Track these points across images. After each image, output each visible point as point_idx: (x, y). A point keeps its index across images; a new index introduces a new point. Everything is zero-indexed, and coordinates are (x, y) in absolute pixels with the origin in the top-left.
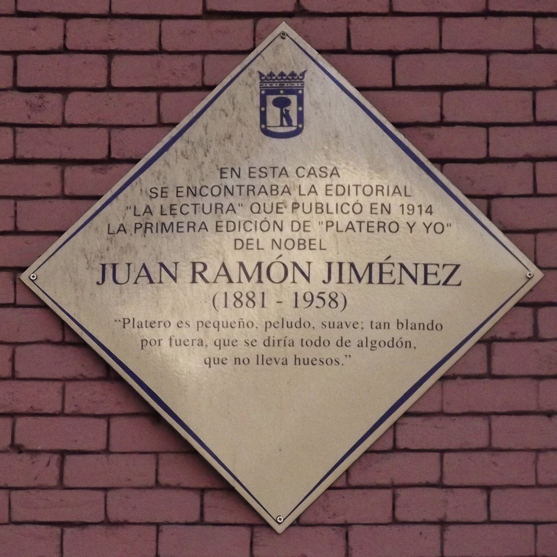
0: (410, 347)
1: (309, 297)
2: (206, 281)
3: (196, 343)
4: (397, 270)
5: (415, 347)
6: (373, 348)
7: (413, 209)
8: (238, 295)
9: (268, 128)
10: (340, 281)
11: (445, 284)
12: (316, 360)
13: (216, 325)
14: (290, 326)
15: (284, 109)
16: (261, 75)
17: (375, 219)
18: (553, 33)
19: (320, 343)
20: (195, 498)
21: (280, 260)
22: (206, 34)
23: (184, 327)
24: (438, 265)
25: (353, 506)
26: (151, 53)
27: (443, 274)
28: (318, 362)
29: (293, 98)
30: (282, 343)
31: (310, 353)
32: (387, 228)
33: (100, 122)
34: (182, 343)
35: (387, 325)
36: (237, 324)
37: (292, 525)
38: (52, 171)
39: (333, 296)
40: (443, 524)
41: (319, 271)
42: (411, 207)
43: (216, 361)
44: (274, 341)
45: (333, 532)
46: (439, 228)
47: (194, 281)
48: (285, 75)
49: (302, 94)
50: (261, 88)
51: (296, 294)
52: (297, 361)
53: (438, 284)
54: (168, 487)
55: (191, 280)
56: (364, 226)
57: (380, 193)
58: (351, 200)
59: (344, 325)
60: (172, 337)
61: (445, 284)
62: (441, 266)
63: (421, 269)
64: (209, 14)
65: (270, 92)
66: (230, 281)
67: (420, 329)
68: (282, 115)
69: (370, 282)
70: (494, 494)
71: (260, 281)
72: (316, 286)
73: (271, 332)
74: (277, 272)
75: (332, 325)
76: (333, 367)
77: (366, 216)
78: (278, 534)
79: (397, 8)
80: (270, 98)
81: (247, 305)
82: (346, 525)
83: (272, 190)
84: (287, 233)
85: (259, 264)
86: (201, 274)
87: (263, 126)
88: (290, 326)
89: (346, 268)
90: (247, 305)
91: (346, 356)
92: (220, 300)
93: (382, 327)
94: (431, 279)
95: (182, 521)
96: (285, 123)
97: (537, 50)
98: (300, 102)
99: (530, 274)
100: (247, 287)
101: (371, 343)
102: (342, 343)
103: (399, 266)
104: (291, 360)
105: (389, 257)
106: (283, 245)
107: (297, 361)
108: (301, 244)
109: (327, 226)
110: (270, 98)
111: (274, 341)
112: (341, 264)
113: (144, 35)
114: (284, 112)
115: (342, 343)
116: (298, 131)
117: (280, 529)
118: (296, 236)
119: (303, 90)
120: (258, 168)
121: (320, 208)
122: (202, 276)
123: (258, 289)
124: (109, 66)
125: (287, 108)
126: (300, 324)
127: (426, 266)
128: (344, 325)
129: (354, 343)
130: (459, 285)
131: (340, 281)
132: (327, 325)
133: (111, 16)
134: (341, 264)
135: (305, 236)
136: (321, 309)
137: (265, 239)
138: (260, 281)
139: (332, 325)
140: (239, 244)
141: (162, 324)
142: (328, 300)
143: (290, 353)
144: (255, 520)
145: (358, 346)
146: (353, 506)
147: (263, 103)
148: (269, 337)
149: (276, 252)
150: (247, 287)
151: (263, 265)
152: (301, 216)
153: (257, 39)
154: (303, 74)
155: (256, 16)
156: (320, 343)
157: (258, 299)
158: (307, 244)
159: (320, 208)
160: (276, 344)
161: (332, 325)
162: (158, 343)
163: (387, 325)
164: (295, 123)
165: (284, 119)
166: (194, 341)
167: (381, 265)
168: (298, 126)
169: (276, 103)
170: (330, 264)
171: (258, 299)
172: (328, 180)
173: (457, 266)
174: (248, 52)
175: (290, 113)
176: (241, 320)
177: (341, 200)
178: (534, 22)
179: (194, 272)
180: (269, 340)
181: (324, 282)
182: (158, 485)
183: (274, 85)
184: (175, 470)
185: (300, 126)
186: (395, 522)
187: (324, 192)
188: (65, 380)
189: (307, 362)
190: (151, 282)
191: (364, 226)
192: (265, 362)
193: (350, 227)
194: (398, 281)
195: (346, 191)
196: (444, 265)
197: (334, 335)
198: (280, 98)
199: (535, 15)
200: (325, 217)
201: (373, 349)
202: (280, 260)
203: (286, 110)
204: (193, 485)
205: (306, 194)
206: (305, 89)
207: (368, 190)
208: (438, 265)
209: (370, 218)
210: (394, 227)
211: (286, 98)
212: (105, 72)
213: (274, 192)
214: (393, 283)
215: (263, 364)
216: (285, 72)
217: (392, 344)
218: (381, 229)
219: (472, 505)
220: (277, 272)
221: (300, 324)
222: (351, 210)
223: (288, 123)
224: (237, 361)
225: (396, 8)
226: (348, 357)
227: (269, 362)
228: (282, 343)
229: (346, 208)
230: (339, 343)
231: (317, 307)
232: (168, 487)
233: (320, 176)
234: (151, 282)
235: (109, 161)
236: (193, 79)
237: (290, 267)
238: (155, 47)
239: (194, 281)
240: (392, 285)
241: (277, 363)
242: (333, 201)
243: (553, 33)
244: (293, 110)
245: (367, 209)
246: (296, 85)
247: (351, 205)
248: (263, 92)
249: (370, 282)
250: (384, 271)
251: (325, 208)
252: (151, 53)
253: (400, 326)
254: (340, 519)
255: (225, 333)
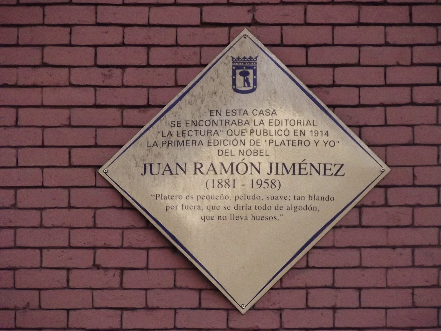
1: (259, 182)
2: (202, 173)
3: (196, 208)
7: (318, 133)
8: (220, 181)
10: (277, 173)
11: (335, 175)
13: (208, 198)
14: (249, 198)
16: (233, 58)
17: (297, 138)
19: (266, 208)
21: (243, 161)
24: (332, 164)
28: (265, 218)
29: (251, 71)
30: (244, 208)
31: (260, 213)
33: (143, 85)
35: (303, 198)
36: (220, 197)
38: (116, 112)
39: (273, 181)
40: (334, 309)
41: (265, 168)
42: (316, 132)
43: (208, 218)
45: (273, 313)
46: (332, 144)
47: (195, 173)
48: (246, 58)
49: (256, 69)
50: (233, 66)
51: (252, 180)
52: (253, 218)
53: (332, 175)
54: (181, 288)
55: (194, 173)
56: (290, 142)
57: (299, 124)
58: (283, 128)
59: (279, 198)
61: (335, 175)
62: (333, 165)
66: (216, 173)
68: (245, 81)
69: (294, 174)
70: (363, 292)
71: (232, 173)
72: (264, 176)
73: (239, 202)
74: (242, 168)
75: (272, 198)
76: (273, 221)
78: (242, 314)
80: (238, 71)
83: (239, 122)
85: (232, 164)
87: (234, 87)
88: (249, 198)
89: (280, 166)
92: (210, 184)
93: (301, 199)
94: (328, 172)
95: (189, 307)
96: (246, 85)
97: (387, 44)
98: (255, 73)
100: (225, 176)
102: (278, 208)
103: (310, 165)
104: (250, 218)
105: (304, 160)
107: (253, 218)
108: (255, 153)
109: (270, 143)
110: (238, 71)
112: (277, 164)
115: (278, 208)
116: (254, 90)
117: (243, 311)
118: (252, 148)
119: (256, 67)
120: (231, 110)
121: (266, 133)
122: (200, 171)
123: (231, 178)
124: (148, 54)
125: (248, 77)
127: (325, 165)
128: (279, 198)
130: (344, 175)
131: (277, 173)
134: (277, 164)
135: (258, 148)
137: (235, 150)
138: (232, 173)
139: (272, 198)
140: (221, 153)
141: (177, 197)
142: (270, 184)
143: (249, 213)
144: (229, 307)
147: (234, 74)
149: (242, 157)
150: (225, 176)
152: (255, 137)
153: (230, 38)
154: (256, 58)
155: (230, 25)
156: (266, 208)
157: (231, 183)
158: (259, 152)
159: (266, 133)
160: (241, 208)
161: (272, 198)
162: (175, 208)
163: (303, 198)
164: (252, 85)
165: (246, 83)
167: (300, 164)
168: (253, 87)
169: (241, 74)
170: (271, 164)
171: (231, 183)
173: (342, 165)
174: (225, 46)
175: (249, 80)
177: (277, 128)
178: (385, 29)
179: (196, 168)
181: (268, 174)
183: (240, 64)
184: (185, 279)
185: (255, 87)
186: (308, 307)
188: (123, 229)
189: (258, 218)
190: (172, 174)
191: (290, 142)
192: (235, 219)
193: (283, 143)
194: (309, 173)
195: (280, 123)
196: (335, 165)
197: (274, 203)
199: (386, 25)
200: (268, 138)
202: (243, 161)
204: (195, 287)
205: (258, 124)
206: (257, 66)
207: (292, 122)
208: (332, 164)
210: (307, 143)
212: (146, 57)
213: (240, 124)
214: (307, 174)
217: (306, 208)
218: (300, 144)
220: (242, 168)
221: (255, 197)
222: (283, 134)
224: (220, 218)
227: (237, 219)
228: (244, 208)
229: (280, 133)
230: (277, 208)
232: (181, 288)
233: (266, 115)
234: (172, 174)
235: (148, 106)
236: (195, 60)
237: (249, 165)
238: (173, 43)
239: (195, 173)
242: (273, 129)
244: (251, 78)
245: (292, 133)
246: (252, 64)
247: (283, 131)
249: (294, 174)
251: (268, 132)
253: (311, 198)
254: (277, 306)
255: (213, 202)
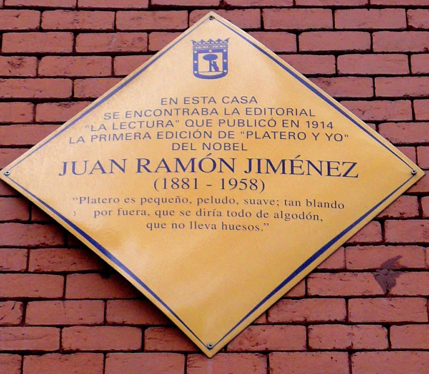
0: (318, 219)
1: (233, 182)
2: (149, 171)
3: (139, 213)
4: (305, 165)
5: (322, 220)
6: (287, 219)
7: (317, 125)
8: (175, 181)
9: (199, 73)
10: (259, 172)
11: (345, 175)
12: (240, 226)
13: (157, 201)
14: (218, 201)
15: (212, 61)
16: (194, 42)
17: (287, 130)
18: (419, 18)
19: (243, 214)
20: (138, 333)
21: (210, 157)
22: (149, 20)
23: (130, 202)
24: (339, 162)
25: (270, 337)
26: (108, 31)
27: (343, 169)
28: (242, 228)
29: (220, 55)
30: (211, 214)
31: (236, 221)
32: (296, 136)
33: (66, 75)
34: (128, 213)
35: (298, 203)
36: (175, 200)
37: (220, 351)
38: (27, 107)
39: (254, 182)
40: (351, 351)
41: (241, 166)
42: (315, 123)
43: (157, 226)
44: (205, 212)
45: (257, 357)
46: (339, 138)
47: (139, 171)
48: (213, 41)
49: (227, 52)
50: (194, 50)
51: (223, 180)
52: (225, 227)
53: (339, 176)
54: (114, 324)
55: (137, 170)
56: (278, 135)
57: (290, 114)
58: (268, 117)
59: (263, 202)
60: (120, 209)
61: (345, 175)
62: (341, 163)
63: (325, 165)
64: (153, 8)
65: (200, 52)
66: (169, 171)
67: (325, 207)
68: (211, 65)
69: (284, 172)
70: (393, 328)
71: (193, 170)
72: (239, 174)
73: (203, 205)
74: (207, 165)
75: (252, 202)
76: (255, 232)
77: (279, 128)
78: (208, 358)
79: (298, 3)
80: (201, 56)
81: (182, 187)
82: (266, 353)
83: (203, 111)
84: (215, 139)
85: (193, 160)
86: (144, 166)
87: (196, 72)
88: (218, 201)
89: (264, 163)
90: (182, 187)
91: (265, 224)
92: (160, 184)
93: (294, 204)
94: (333, 172)
95: (126, 349)
96: (213, 69)
97: (409, 28)
98: (225, 56)
99: (414, 171)
100: (181, 175)
101: (286, 215)
102: (261, 215)
103: (307, 162)
104: (219, 226)
105: (299, 156)
106: (212, 147)
107: (225, 227)
108: (227, 147)
109: (248, 135)
110: (201, 56)
111: (205, 212)
112: (259, 161)
113: (103, 20)
114: (213, 63)
115: (261, 215)
116: (223, 75)
117: (209, 353)
118: (222, 141)
119: (227, 50)
120: (191, 98)
121: (241, 123)
122: (146, 168)
123: (192, 176)
124: (75, 40)
125: (215, 61)
126: (226, 200)
127: (329, 163)
128: (263, 202)
129: (271, 215)
130: (357, 177)
131: (259, 172)
132: (249, 202)
133: (77, 9)
134: (259, 161)
135: (231, 141)
136: (244, 191)
137: (198, 144)
138: (193, 170)
139: (252, 202)
140: (176, 147)
141: (112, 201)
142: (249, 184)
143: (218, 221)
144: (188, 349)
145: (275, 217)
146: (270, 337)
147: (196, 57)
148: (201, 209)
149: (207, 151)
150: (181, 175)
151: (195, 160)
152: (225, 128)
153: (190, 23)
154: (227, 40)
155: (190, 9)
156: (243, 214)
157: (192, 183)
158: (232, 146)
159: (241, 123)
160: (207, 214)
161: (252, 202)
162: (108, 213)
163: (298, 203)
164: (221, 69)
165: (212, 67)
166: (138, 212)
167: (292, 161)
168: (223, 71)
169: (205, 58)
170: (250, 160)
171: (192, 183)
172: (247, 105)
173: (354, 164)
174: (183, 31)
175: (217, 64)
176: (177, 197)
177: (258, 118)
178: (406, 11)
179: (139, 165)
180: (201, 211)
181: (246, 172)
182: (105, 323)
183: (205, 47)
184: (120, 311)
185: (225, 71)
186: (309, 349)
187: (245, 112)
188: (29, 248)
189: (232, 228)
190: (104, 172)
191: (278, 135)
192: (197, 227)
193: (266, 135)
194: (306, 173)
195: (263, 111)
196: (344, 163)
197: (255, 209)
198: (210, 54)
199: (407, 8)
200: (246, 129)
201: (286, 219)
202: (210, 157)
203: (213, 62)
204: (135, 323)
205: (231, 113)
206: (229, 49)
207: (280, 112)
208: (339, 162)
209: (283, 129)
210: (301, 136)
211: (213, 55)
212: (71, 43)
213: (204, 113)
214: (303, 174)
215: (196, 228)
216: (213, 39)
217: (304, 216)
218: (292, 138)
219: (375, 337)
220: (207, 165)
221: (226, 200)
222: (267, 125)
223: (215, 69)
224: (174, 226)
225: (297, 4)
226: (266, 225)
227: (201, 227)
228: (211, 214)
229: (262, 123)
230: (259, 215)
231: (240, 189)
232: (114, 324)
233: (242, 102)
234: (104, 172)
235: (73, 99)
236: (141, 47)
237: (218, 162)
238: (111, 27)
239: (139, 171)
240: (302, 175)
241: (207, 228)
242: (252, 119)
243: (419, 18)
244: (219, 62)
245: (279, 124)
246: (222, 46)
247: (267, 121)
248: (196, 52)
249: (284, 172)
250: (294, 165)
251: (246, 123)
252: (108, 31)
253: (309, 204)
254: (262, 347)
255: (164, 207)
